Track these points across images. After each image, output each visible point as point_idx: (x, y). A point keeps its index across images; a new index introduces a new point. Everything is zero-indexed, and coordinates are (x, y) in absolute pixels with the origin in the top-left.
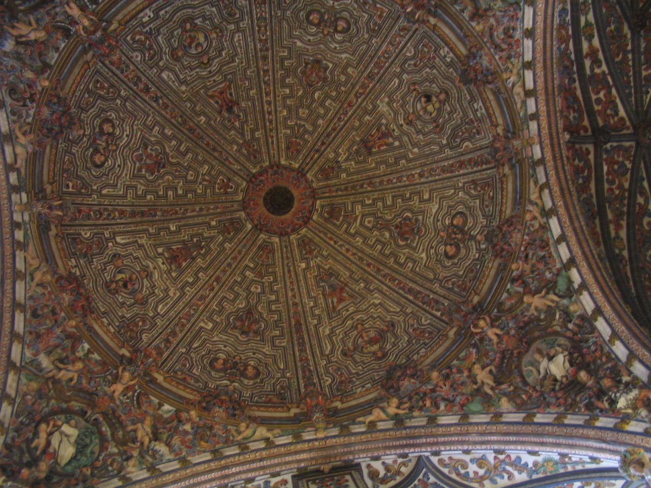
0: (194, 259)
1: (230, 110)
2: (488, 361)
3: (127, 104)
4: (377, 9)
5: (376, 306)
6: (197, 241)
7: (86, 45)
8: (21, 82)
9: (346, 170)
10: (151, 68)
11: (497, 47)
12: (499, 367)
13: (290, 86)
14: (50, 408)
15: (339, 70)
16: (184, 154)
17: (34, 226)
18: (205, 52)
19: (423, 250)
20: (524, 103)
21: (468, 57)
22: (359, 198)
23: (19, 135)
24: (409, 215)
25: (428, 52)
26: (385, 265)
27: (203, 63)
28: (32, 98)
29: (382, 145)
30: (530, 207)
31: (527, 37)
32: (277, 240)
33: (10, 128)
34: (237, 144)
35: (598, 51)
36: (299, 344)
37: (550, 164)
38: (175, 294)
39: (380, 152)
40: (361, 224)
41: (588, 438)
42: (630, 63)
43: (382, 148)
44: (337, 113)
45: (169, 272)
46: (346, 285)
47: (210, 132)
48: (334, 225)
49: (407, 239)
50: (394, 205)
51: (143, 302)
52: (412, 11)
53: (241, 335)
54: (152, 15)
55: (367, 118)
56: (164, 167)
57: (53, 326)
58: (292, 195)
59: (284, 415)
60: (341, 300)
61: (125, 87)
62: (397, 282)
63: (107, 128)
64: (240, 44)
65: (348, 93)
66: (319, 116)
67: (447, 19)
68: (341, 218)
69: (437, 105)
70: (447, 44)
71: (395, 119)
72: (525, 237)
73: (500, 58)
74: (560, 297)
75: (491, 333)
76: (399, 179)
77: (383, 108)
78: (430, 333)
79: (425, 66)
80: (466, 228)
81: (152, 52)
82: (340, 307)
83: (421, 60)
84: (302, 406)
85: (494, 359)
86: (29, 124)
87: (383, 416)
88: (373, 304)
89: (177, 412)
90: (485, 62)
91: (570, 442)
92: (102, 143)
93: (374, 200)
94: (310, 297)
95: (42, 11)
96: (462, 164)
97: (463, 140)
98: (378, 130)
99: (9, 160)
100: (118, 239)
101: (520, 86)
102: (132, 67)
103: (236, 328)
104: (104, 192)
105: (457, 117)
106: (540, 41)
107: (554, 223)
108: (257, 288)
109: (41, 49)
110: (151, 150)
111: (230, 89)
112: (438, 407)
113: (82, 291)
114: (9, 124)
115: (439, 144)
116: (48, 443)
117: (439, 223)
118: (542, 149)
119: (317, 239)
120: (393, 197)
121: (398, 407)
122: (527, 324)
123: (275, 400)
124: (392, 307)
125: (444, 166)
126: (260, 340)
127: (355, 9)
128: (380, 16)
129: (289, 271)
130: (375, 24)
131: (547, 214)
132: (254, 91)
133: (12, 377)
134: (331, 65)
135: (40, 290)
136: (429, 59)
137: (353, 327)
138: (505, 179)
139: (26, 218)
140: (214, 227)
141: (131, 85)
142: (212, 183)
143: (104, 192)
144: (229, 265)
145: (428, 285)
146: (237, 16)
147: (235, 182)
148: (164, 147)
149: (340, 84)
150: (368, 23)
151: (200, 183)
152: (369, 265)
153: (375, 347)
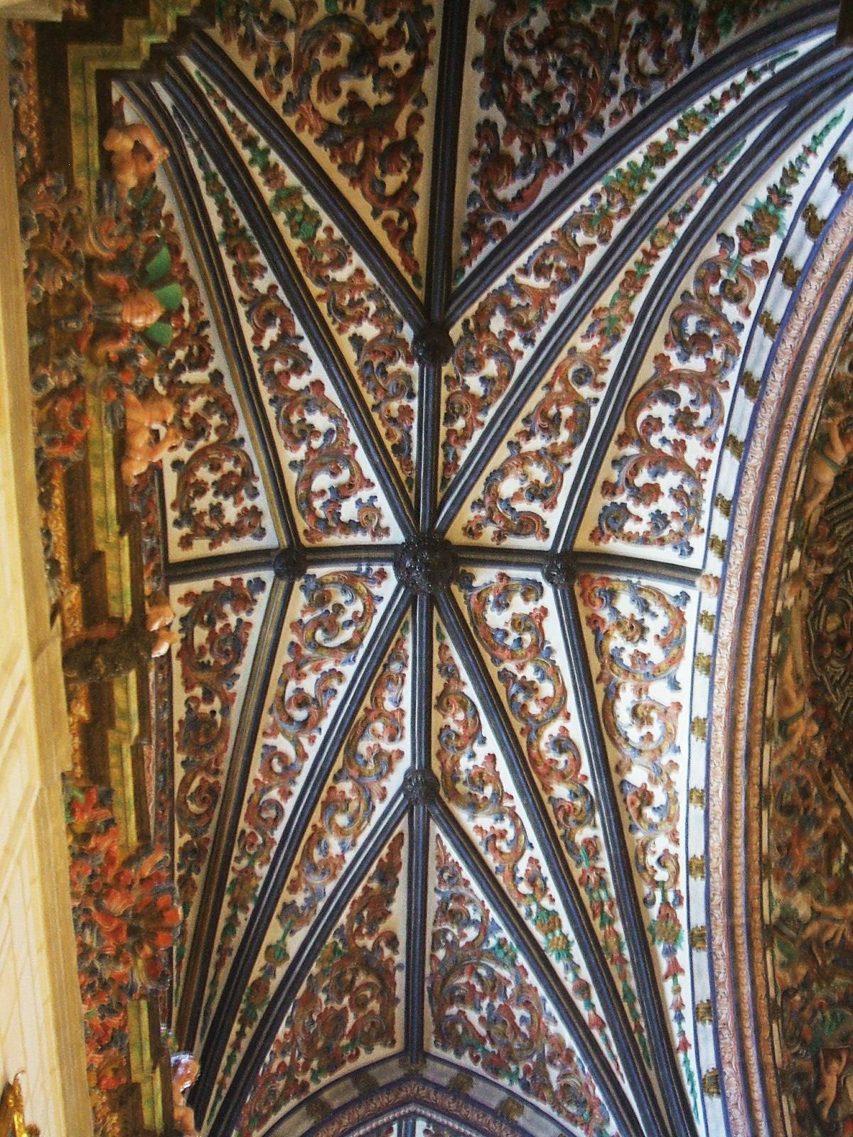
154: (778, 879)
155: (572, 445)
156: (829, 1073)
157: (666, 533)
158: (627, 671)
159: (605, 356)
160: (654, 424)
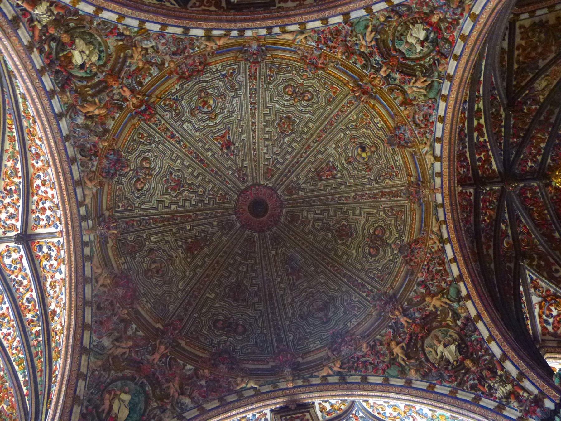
0: (202, 248)
1: (228, 148)
2: (401, 339)
3: (159, 146)
4: (333, 88)
5: (322, 284)
6: (204, 236)
7: (133, 113)
8: (88, 143)
9: (304, 189)
10: (176, 122)
11: (417, 125)
12: (408, 345)
14: (111, 378)
16: (197, 177)
17: (97, 243)
18: (213, 111)
19: (354, 248)
20: (433, 164)
21: (395, 128)
23: (87, 182)
24: (345, 223)
25: (366, 119)
26: (328, 256)
27: (211, 118)
28: (96, 155)
29: (329, 175)
30: (433, 237)
31: (440, 122)
32: (257, 235)
33: (80, 176)
34: (233, 170)
35: (483, 126)
36: (271, 308)
37: (448, 208)
38: (190, 274)
39: (327, 179)
40: (313, 226)
41: (474, 412)
42: (503, 134)
43: (329, 177)
45: (185, 258)
46: (302, 268)
47: (215, 161)
48: (295, 226)
49: (343, 239)
50: (335, 215)
51: (170, 283)
52: (359, 95)
54: (178, 88)
55: (320, 156)
56: (183, 186)
57: (112, 314)
58: (267, 205)
60: (299, 278)
61: (158, 135)
62: (336, 268)
63: (145, 165)
64: (237, 105)
65: (308, 140)
68: (299, 222)
69: (369, 154)
70: (380, 117)
71: (339, 160)
72: (428, 255)
73: (419, 133)
74: (451, 301)
76: (340, 198)
77: (331, 151)
78: (359, 308)
80: (384, 238)
81: (177, 111)
82: (298, 282)
83: (360, 123)
84: (277, 361)
85: (405, 339)
86: (93, 172)
87: (331, 372)
89: (196, 370)
91: (461, 411)
92: (141, 175)
93: (322, 210)
94: (278, 275)
95: (103, 94)
96: (383, 194)
97: (385, 179)
98: (327, 165)
99: (80, 197)
100: (152, 239)
101: (431, 154)
102: (163, 122)
103: (230, 297)
104: (143, 207)
105: (383, 163)
106: (448, 126)
107: (448, 248)
108: (243, 268)
109: (102, 120)
110: (175, 175)
111: (229, 134)
112: (367, 370)
113: (131, 285)
114: (80, 173)
116: (111, 407)
117: (365, 231)
118: (443, 197)
120: (335, 210)
121: (340, 368)
122: (427, 316)
123: (257, 351)
124: (333, 286)
125: (371, 194)
127: (317, 86)
128: (335, 93)
129: (265, 256)
130: (331, 97)
132: (245, 136)
133: (84, 358)
134: (298, 121)
135: (102, 289)
136: (366, 123)
137: (307, 298)
138: (414, 212)
139: (92, 238)
140: (215, 226)
141: (163, 133)
142: (214, 197)
143: (143, 207)
144: (225, 252)
146: (237, 87)
147: (230, 195)
148: (183, 173)
149: (303, 133)
151: (207, 197)
152: (317, 255)
153: (321, 314)
154: (95, 333)
155: (18, 200)
157: (50, 223)
158: (48, 272)
159: (17, 167)
160: (38, 187)
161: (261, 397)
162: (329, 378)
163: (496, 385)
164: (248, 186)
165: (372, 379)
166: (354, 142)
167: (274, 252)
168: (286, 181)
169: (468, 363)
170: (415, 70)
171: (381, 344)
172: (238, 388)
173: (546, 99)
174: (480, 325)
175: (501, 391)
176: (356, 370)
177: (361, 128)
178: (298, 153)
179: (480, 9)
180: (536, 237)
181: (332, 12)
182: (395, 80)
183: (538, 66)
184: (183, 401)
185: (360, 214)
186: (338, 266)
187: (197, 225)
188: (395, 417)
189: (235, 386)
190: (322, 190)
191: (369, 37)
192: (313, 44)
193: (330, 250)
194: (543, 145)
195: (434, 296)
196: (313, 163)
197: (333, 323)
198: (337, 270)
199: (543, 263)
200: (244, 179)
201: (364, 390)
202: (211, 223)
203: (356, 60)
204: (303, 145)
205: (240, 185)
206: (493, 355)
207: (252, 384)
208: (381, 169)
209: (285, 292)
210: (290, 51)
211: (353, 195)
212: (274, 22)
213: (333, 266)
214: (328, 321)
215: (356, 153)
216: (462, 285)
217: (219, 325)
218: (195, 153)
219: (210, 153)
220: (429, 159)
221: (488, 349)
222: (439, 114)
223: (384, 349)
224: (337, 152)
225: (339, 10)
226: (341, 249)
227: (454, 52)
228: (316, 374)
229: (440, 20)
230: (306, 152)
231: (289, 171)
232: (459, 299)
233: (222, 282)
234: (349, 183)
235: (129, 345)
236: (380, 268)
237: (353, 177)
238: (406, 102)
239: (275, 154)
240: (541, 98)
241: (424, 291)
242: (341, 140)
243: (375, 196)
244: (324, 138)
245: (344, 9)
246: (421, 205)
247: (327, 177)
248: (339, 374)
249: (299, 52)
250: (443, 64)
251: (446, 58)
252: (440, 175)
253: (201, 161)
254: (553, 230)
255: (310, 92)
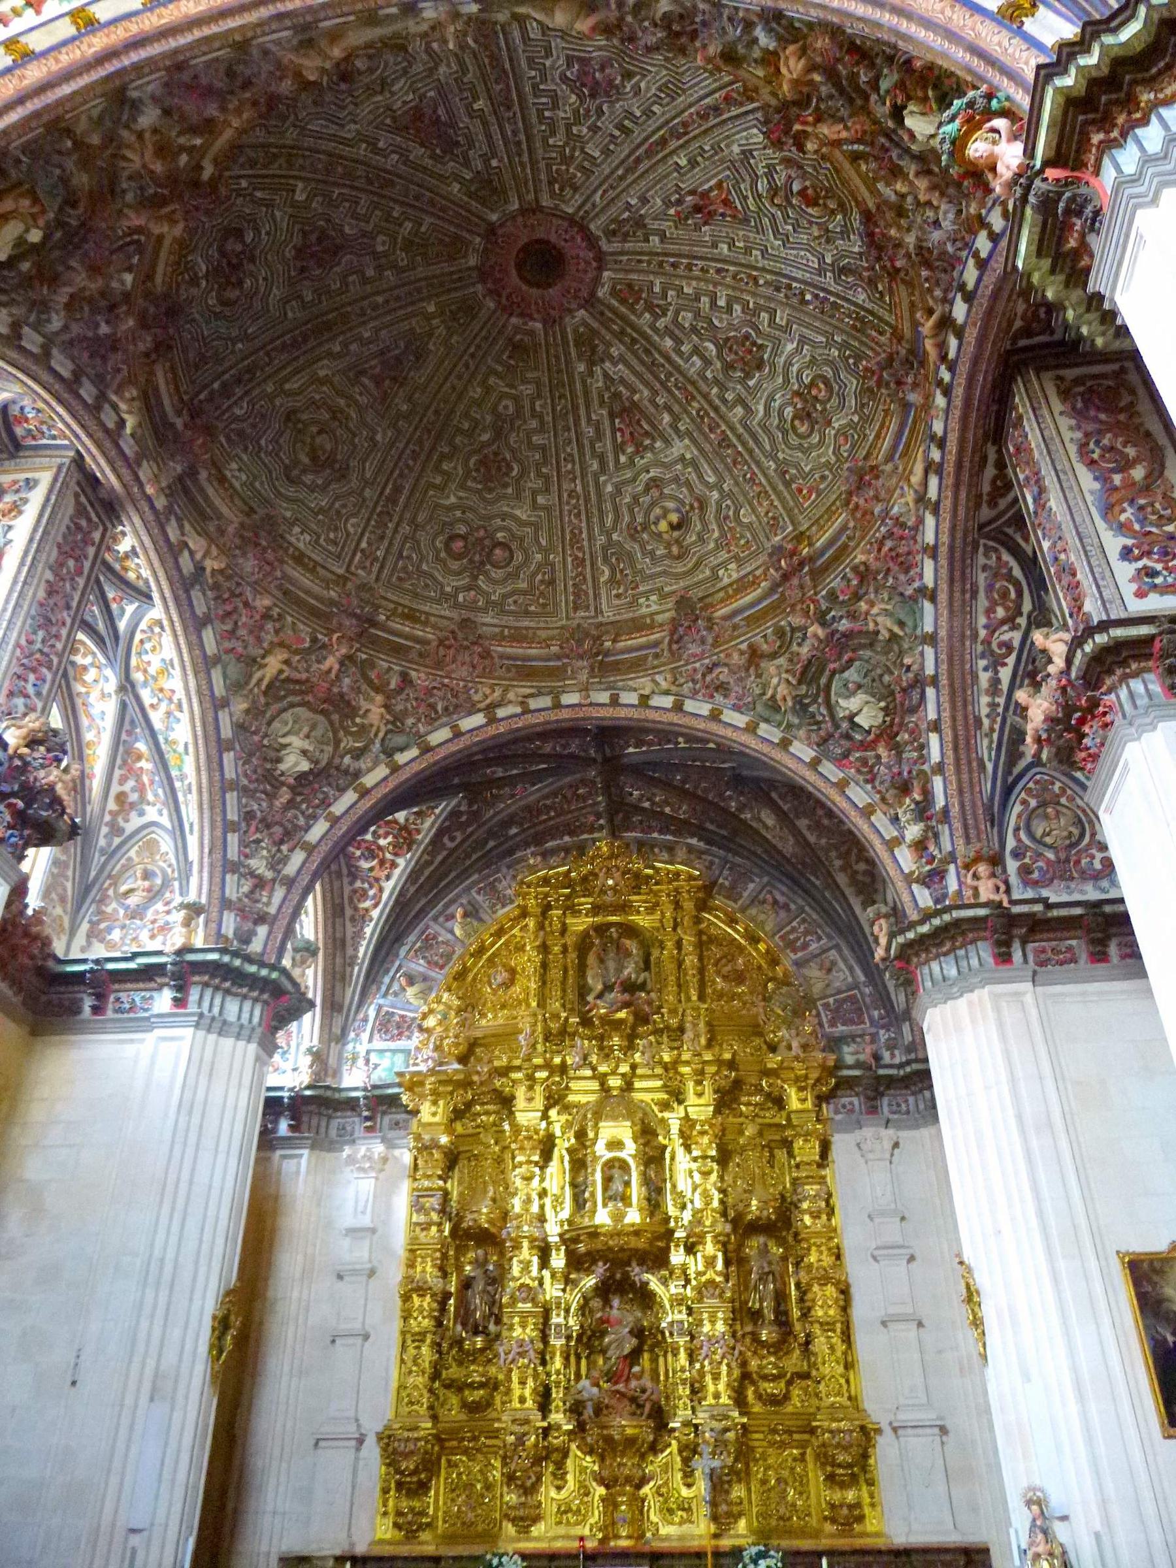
1: (697, 209)
9: (591, 374)
11: (710, 670)
12: (288, 680)
13: (729, 309)
15: (744, 394)
19: (461, 498)
21: (710, 619)
22: (546, 391)
24: (514, 473)
27: (775, 194)
31: (712, 711)
39: (614, 430)
40: (503, 396)
44: (681, 373)
46: (401, 385)
48: (503, 352)
50: (531, 446)
52: (781, 568)
53: (294, 247)
58: (549, 286)
59: (168, 409)
60: (378, 380)
62: (411, 463)
65: (706, 396)
66: (678, 342)
67: (765, 604)
71: (658, 463)
73: (695, 670)
74: (383, 740)
75: (331, 662)
76: (570, 458)
77: (680, 447)
79: (723, 535)
82: (366, 381)
87: (198, 556)
88: (375, 432)
89: (127, 296)
90: (694, 649)
91: (205, 806)
94: (377, 330)
97: (613, 570)
98: (647, 434)
107: (478, 719)
108: (384, 243)
115: (614, 528)
119: (476, 325)
120: (543, 449)
122: (348, 703)
126: (290, 277)
127: (819, 456)
131: (490, 709)
137: (335, 413)
142: (567, 160)
145: (407, 515)
149: (723, 388)
150: (797, 466)
156: (16, 200)
161: (108, 444)
162: (186, 553)
163: (265, 852)
164: (598, 238)
165: (208, 636)
166: (692, 506)
167: (431, 309)
168: (612, 332)
169: (285, 796)
170: (809, 684)
171: (277, 632)
172: (114, 398)
173: (744, 822)
174: (350, 797)
175: (258, 864)
176: (215, 599)
177: (720, 526)
178: (678, 368)
179: (878, 825)
180: (508, 806)
181: (944, 572)
182: (799, 645)
183: (798, 818)
184: (54, 317)
185: (535, 506)
186: (418, 468)
187: (485, 124)
188: (145, 671)
189: (115, 386)
190: (589, 419)
191: (886, 625)
192: (896, 510)
193: (451, 443)
194: (667, 810)
195: (386, 706)
196: (653, 402)
197: (291, 491)
198: (408, 466)
199: (464, 818)
200: (614, 233)
201: (185, 629)
202: (494, 155)
203: (849, 581)
204: (693, 383)
205: (602, 220)
206: (307, 828)
207: (130, 422)
208: (632, 565)
209: (339, 356)
210: (894, 447)
211: (579, 488)
212: (952, 458)
213: (415, 456)
214: (292, 481)
215: (671, 505)
216: (414, 752)
217: (233, 246)
218: (686, 133)
219: (683, 162)
220: (645, 684)
221: (315, 817)
222: (725, 711)
223: (269, 637)
224: (676, 462)
225: (944, 586)
226: (455, 468)
227: (825, 762)
228: (187, 527)
229: (878, 757)
230: (679, 389)
231: (634, 341)
232: (389, 753)
233: (337, 207)
234: (605, 482)
235: (152, 167)
236: (424, 567)
237: (618, 491)
238: (754, 656)
239: (677, 313)
240: (747, 816)
241: (393, 686)
242: (700, 477)
243: (576, 538)
244: (707, 438)
245: (943, 597)
246: (558, 657)
247: (620, 430)
248: (200, 569)
249: (888, 467)
250: (809, 738)
251: (818, 745)
252: (615, 702)
253: (663, 142)
254: (521, 824)
255: (809, 436)
